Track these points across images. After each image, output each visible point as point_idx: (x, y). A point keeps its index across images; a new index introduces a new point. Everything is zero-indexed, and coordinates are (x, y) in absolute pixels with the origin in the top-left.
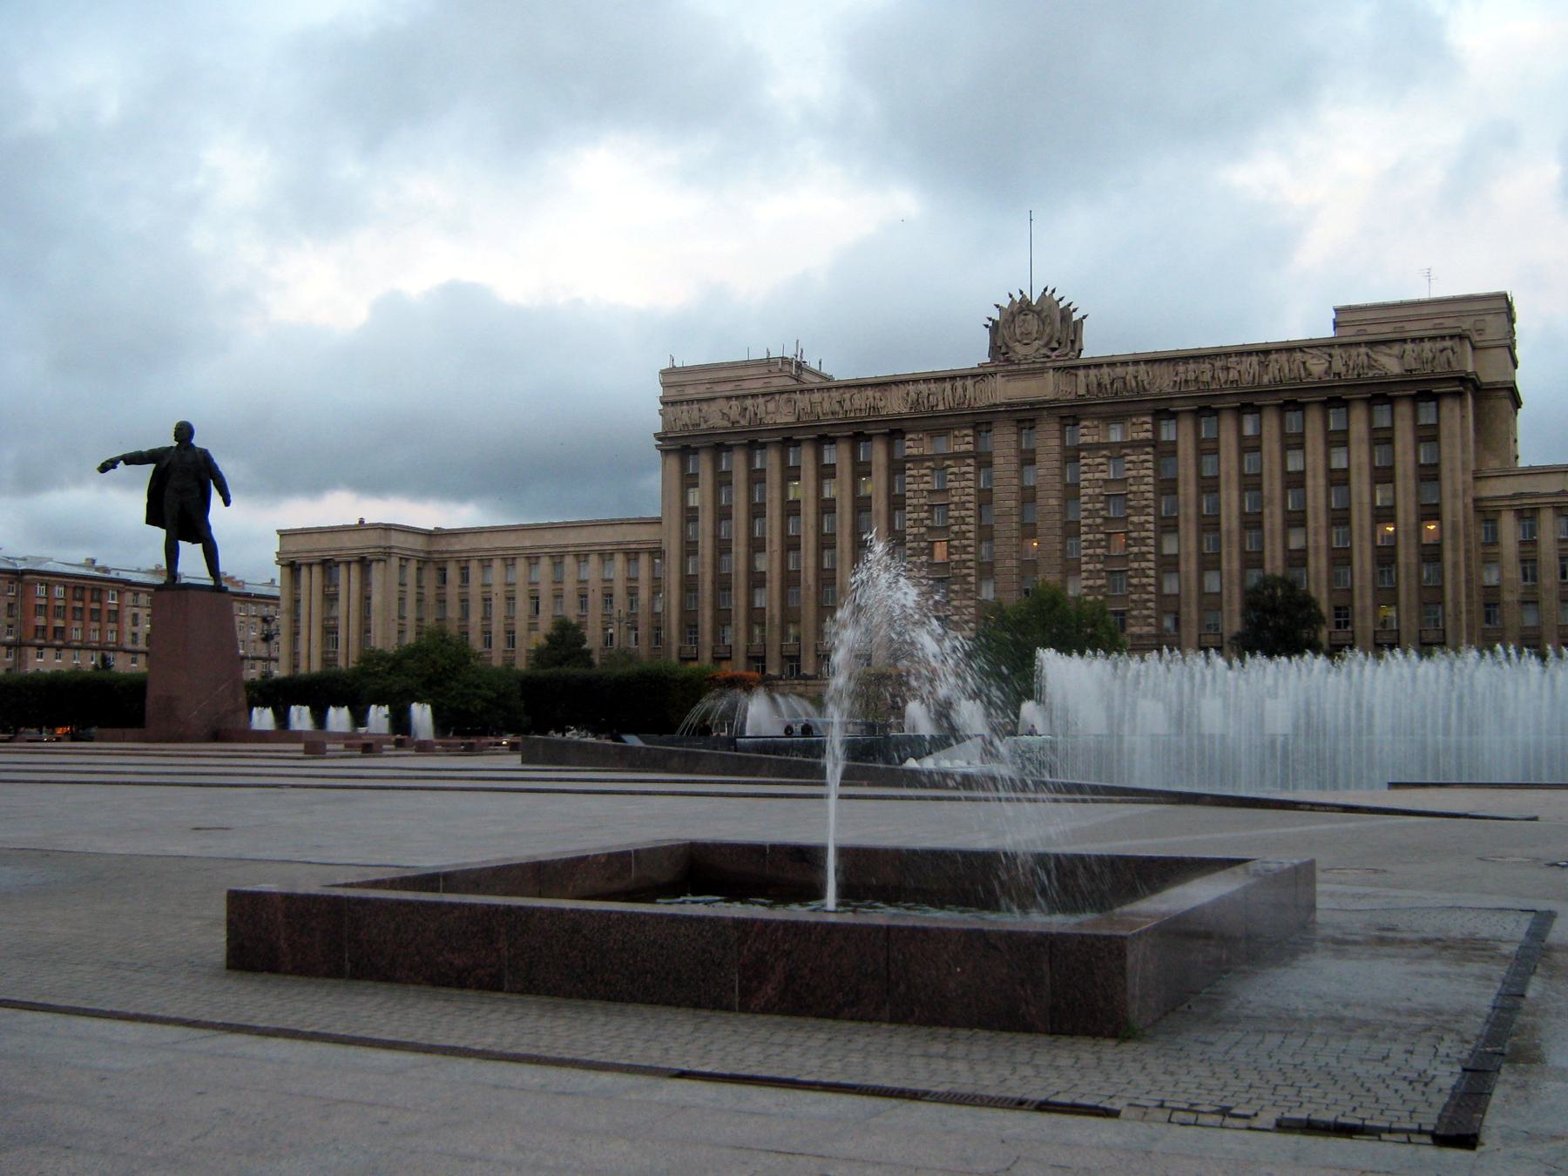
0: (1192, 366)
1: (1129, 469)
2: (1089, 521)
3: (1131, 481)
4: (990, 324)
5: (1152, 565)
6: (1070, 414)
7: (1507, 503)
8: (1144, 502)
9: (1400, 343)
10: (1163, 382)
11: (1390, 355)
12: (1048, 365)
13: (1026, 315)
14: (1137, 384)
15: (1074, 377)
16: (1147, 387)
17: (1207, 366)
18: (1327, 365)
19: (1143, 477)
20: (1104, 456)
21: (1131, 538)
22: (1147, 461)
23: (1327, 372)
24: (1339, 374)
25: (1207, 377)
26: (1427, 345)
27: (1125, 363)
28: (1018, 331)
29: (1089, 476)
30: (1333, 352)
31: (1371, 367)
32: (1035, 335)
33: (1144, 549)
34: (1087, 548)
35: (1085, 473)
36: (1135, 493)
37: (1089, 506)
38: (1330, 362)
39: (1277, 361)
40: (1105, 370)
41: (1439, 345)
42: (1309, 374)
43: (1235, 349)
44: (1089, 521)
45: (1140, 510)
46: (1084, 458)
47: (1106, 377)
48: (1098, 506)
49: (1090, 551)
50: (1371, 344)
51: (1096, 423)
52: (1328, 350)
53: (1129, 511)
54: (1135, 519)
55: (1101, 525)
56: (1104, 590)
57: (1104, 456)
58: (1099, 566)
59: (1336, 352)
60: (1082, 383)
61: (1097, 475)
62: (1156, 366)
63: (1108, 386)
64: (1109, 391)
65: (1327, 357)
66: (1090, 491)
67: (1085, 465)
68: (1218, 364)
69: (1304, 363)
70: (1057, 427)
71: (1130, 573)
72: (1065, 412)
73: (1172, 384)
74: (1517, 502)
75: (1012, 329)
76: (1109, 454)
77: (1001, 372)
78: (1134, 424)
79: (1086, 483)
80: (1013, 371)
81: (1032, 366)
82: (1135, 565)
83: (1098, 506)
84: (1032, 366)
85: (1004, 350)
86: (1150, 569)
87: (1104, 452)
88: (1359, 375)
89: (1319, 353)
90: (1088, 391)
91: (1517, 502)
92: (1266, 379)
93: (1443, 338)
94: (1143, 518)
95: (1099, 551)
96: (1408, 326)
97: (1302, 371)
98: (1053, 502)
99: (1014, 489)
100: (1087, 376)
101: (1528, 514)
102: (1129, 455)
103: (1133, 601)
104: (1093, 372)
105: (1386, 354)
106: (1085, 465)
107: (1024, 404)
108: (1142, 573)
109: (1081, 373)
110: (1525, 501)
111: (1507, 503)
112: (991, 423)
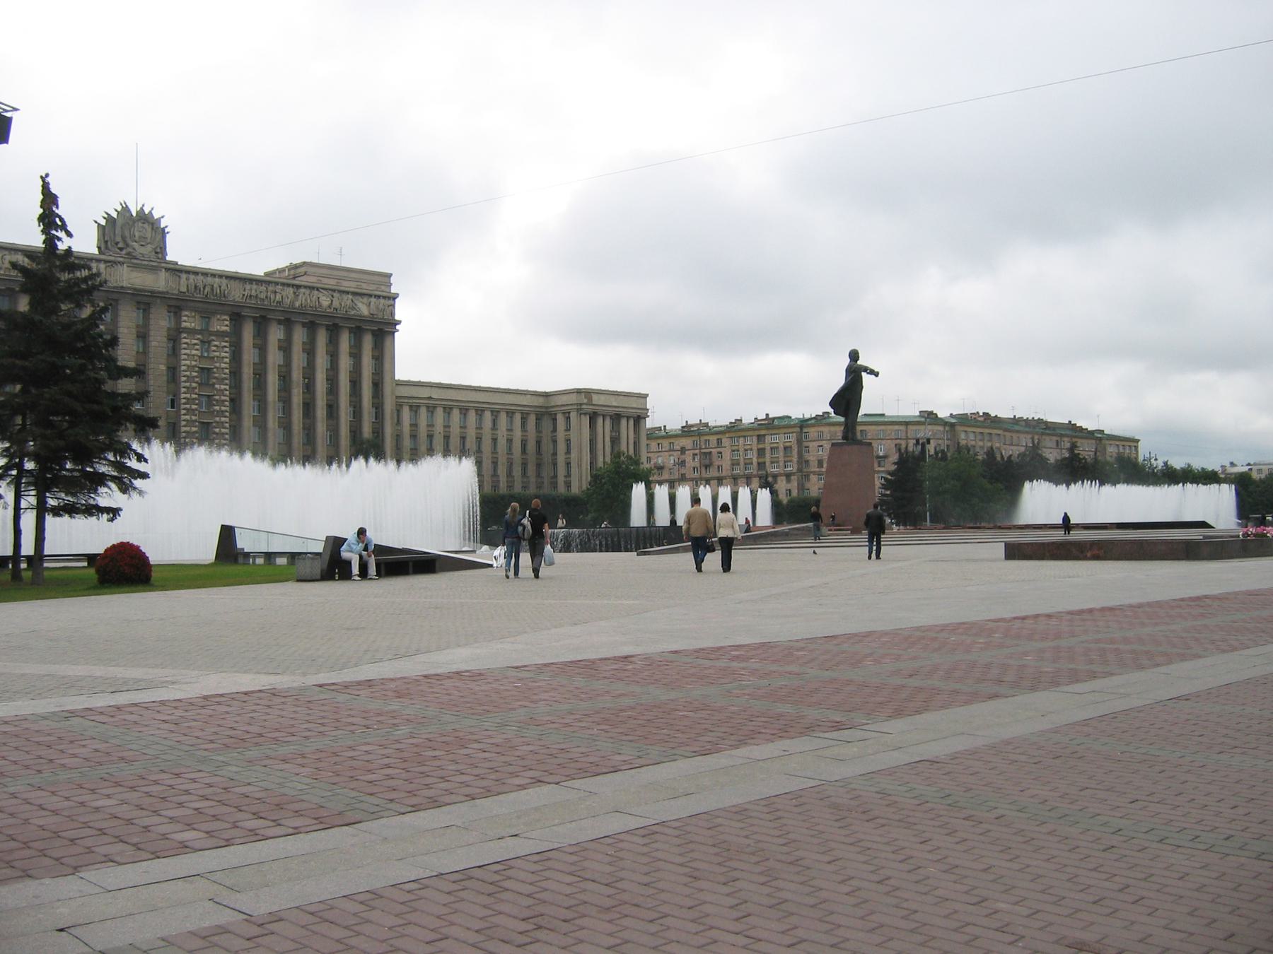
0: (254, 286)
1: (214, 351)
2: (188, 384)
4: (103, 222)
5: (227, 420)
6: (176, 305)
7: (406, 401)
9: (367, 297)
10: (236, 294)
12: (163, 265)
13: (144, 223)
14: (220, 291)
15: (178, 278)
17: (263, 288)
18: (330, 302)
19: (223, 357)
21: (215, 400)
22: (225, 347)
23: (330, 307)
25: (263, 296)
26: (382, 301)
27: (213, 275)
28: (137, 234)
29: (188, 351)
30: (334, 294)
31: (353, 308)
32: (149, 241)
33: (223, 408)
35: (184, 349)
36: (217, 368)
37: (188, 373)
38: (332, 301)
39: (304, 294)
40: (200, 277)
42: (320, 306)
43: (219, 272)
44: (188, 384)
45: (221, 381)
46: (185, 338)
49: (188, 406)
50: (355, 294)
51: (193, 314)
52: (332, 293)
53: (214, 381)
54: (217, 386)
55: (196, 388)
57: (198, 339)
60: (184, 284)
62: (232, 282)
63: (202, 289)
64: (202, 293)
65: (330, 296)
67: (184, 343)
68: (271, 288)
70: (165, 312)
71: (214, 424)
72: (173, 303)
73: (241, 296)
74: (411, 401)
75: (132, 230)
78: (218, 320)
80: (138, 264)
81: (151, 263)
82: (217, 419)
83: (195, 374)
84: (151, 263)
85: (120, 245)
87: (199, 336)
88: (346, 311)
89: (326, 293)
90: (188, 290)
91: (411, 401)
92: (297, 304)
94: (223, 387)
96: (345, 284)
97: (317, 303)
98: (163, 367)
99: (134, 353)
100: (188, 279)
101: (414, 409)
102: (214, 340)
104: (192, 277)
105: (361, 302)
106: (184, 343)
107: (146, 291)
108: (221, 424)
109: (184, 276)
110: (415, 401)
111: (406, 401)
112: (116, 301)
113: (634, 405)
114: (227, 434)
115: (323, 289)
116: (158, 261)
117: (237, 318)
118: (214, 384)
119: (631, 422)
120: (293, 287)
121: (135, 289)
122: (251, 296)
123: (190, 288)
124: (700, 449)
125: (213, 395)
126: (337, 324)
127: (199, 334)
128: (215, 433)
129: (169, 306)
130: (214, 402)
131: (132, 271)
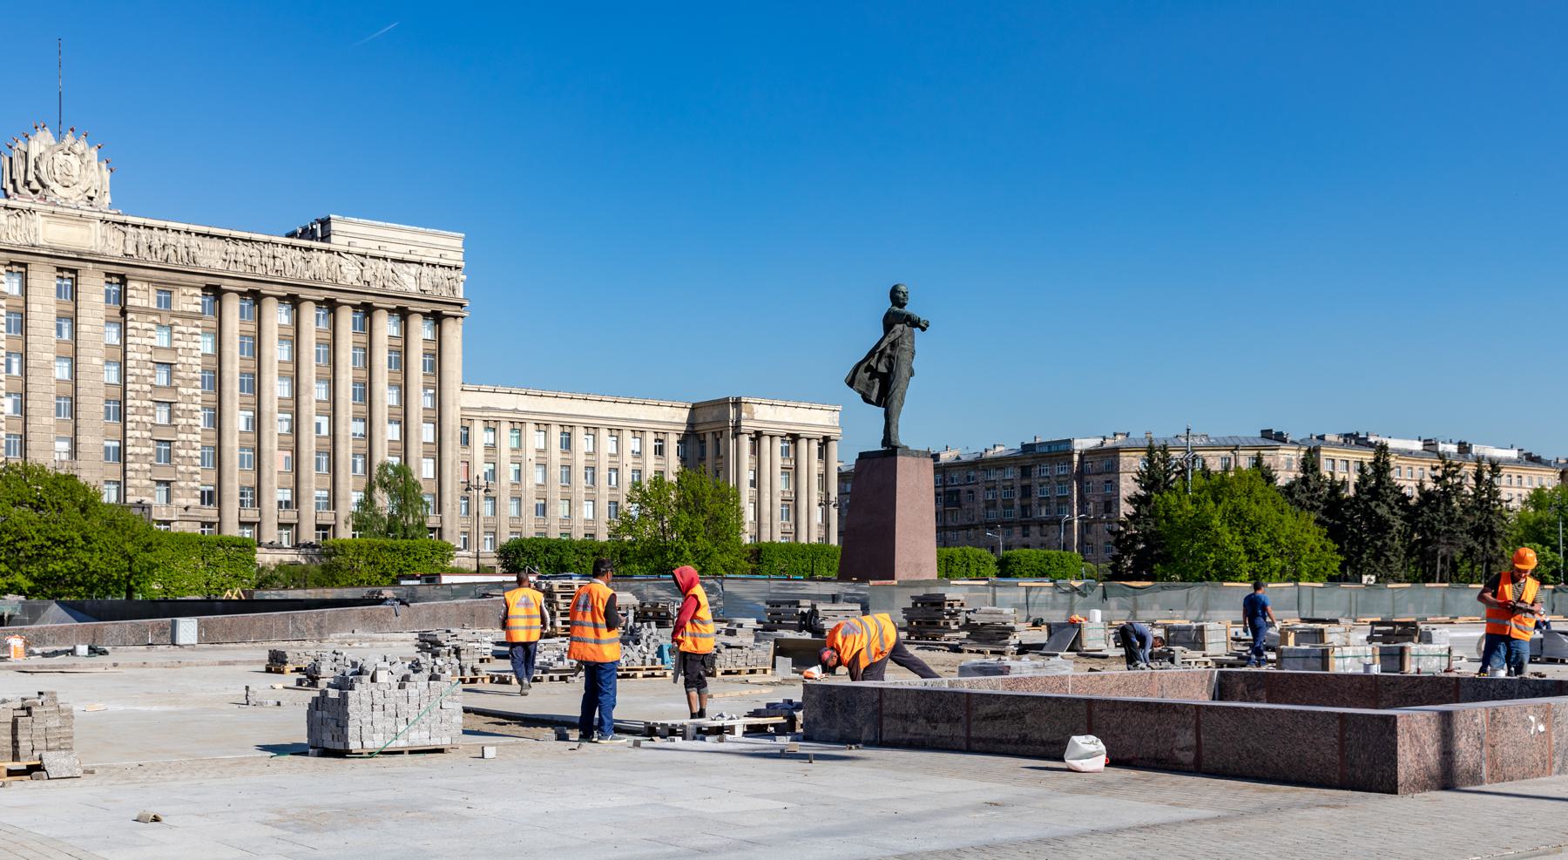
0: (242, 248)
3: (180, 351)
5: (198, 438)
7: (479, 414)
8: (192, 375)
9: (416, 265)
11: (409, 274)
14: (188, 254)
15: (122, 235)
16: (197, 260)
17: (255, 252)
18: (359, 272)
20: (153, 322)
24: (368, 282)
25: (256, 261)
26: (439, 271)
29: (138, 340)
34: (133, 414)
41: (447, 273)
47: (157, 241)
48: (146, 372)
50: (394, 260)
51: (145, 286)
52: (362, 259)
53: (178, 382)
56: (151, 458)
57: (153, 322)
58: (147, 434)
59: (368, 261)
61: (145, 341)
64: (159, 255)
66: (138, 356)
68: (268, 250)
69: (340, 266)
74: (485, 414)
76: (158, 321)
77: (40, 210)
78: (184, 295)
79: (134, 347)
82: (183, 436)
86: (197, 442)
88: (384, 286)
91: (485, 414)
93: (450, 267)
94: (191, 391)
95: (145, 419)
102: (178, 325)
103: (182, 473)
106: (132, 328)
108: (189, 444)
109: (130, 230)
110: (491, 414)
111: (479, 414)
113: (820, 422)
114: (198, 457)
115: (348, 253)
116: (90, 208)
117: (216, 293)
118: (176, 387)
119: (815, 446)
120: (300, 250)
121: (55, 250)
122: (236, 262)
123: (140, 251)
124: (945, 486)
125: (176, 403)
126: (297, 296)
127: (156, 314)
128: (178, 456)
129: (108, 275)
130: (179, 413)
131: (48, 222)
